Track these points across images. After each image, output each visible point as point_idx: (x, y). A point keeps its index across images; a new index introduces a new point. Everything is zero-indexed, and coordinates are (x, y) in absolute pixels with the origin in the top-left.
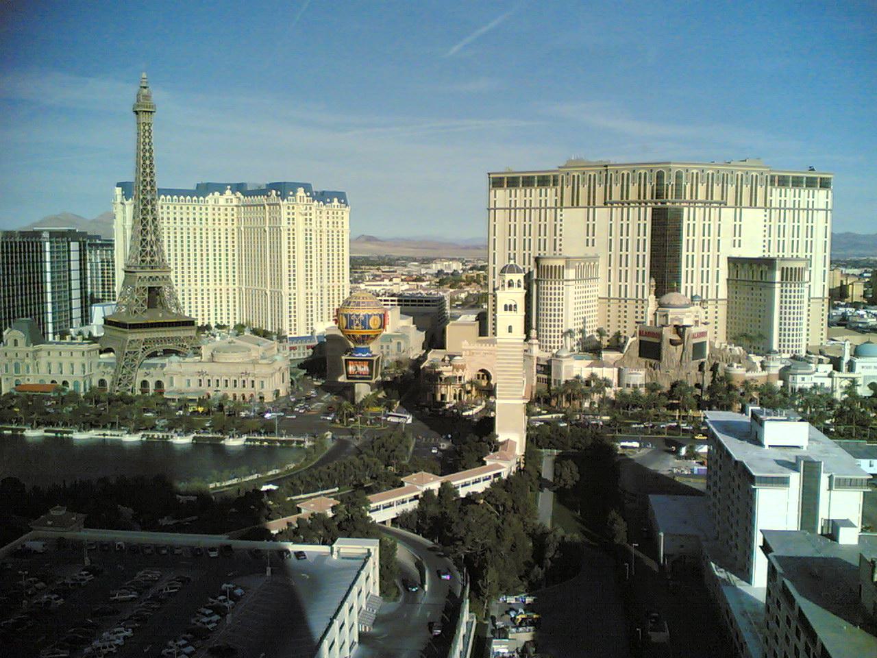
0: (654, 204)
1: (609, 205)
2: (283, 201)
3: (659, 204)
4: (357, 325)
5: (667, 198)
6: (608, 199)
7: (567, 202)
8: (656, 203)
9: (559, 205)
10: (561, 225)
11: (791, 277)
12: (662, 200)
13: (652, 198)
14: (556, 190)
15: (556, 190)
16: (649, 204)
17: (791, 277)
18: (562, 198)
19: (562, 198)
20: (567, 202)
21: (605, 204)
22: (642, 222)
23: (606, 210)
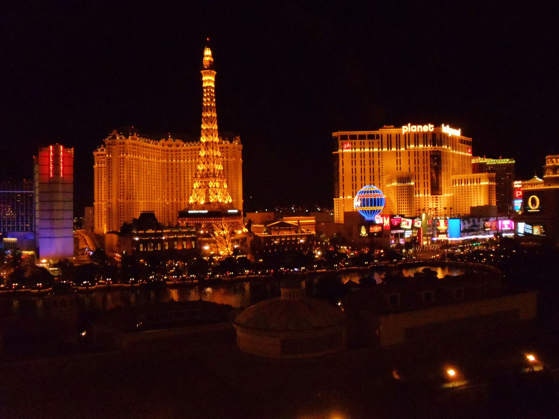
12: (435, 147)
14: (379, 142)
15: (379, 142)
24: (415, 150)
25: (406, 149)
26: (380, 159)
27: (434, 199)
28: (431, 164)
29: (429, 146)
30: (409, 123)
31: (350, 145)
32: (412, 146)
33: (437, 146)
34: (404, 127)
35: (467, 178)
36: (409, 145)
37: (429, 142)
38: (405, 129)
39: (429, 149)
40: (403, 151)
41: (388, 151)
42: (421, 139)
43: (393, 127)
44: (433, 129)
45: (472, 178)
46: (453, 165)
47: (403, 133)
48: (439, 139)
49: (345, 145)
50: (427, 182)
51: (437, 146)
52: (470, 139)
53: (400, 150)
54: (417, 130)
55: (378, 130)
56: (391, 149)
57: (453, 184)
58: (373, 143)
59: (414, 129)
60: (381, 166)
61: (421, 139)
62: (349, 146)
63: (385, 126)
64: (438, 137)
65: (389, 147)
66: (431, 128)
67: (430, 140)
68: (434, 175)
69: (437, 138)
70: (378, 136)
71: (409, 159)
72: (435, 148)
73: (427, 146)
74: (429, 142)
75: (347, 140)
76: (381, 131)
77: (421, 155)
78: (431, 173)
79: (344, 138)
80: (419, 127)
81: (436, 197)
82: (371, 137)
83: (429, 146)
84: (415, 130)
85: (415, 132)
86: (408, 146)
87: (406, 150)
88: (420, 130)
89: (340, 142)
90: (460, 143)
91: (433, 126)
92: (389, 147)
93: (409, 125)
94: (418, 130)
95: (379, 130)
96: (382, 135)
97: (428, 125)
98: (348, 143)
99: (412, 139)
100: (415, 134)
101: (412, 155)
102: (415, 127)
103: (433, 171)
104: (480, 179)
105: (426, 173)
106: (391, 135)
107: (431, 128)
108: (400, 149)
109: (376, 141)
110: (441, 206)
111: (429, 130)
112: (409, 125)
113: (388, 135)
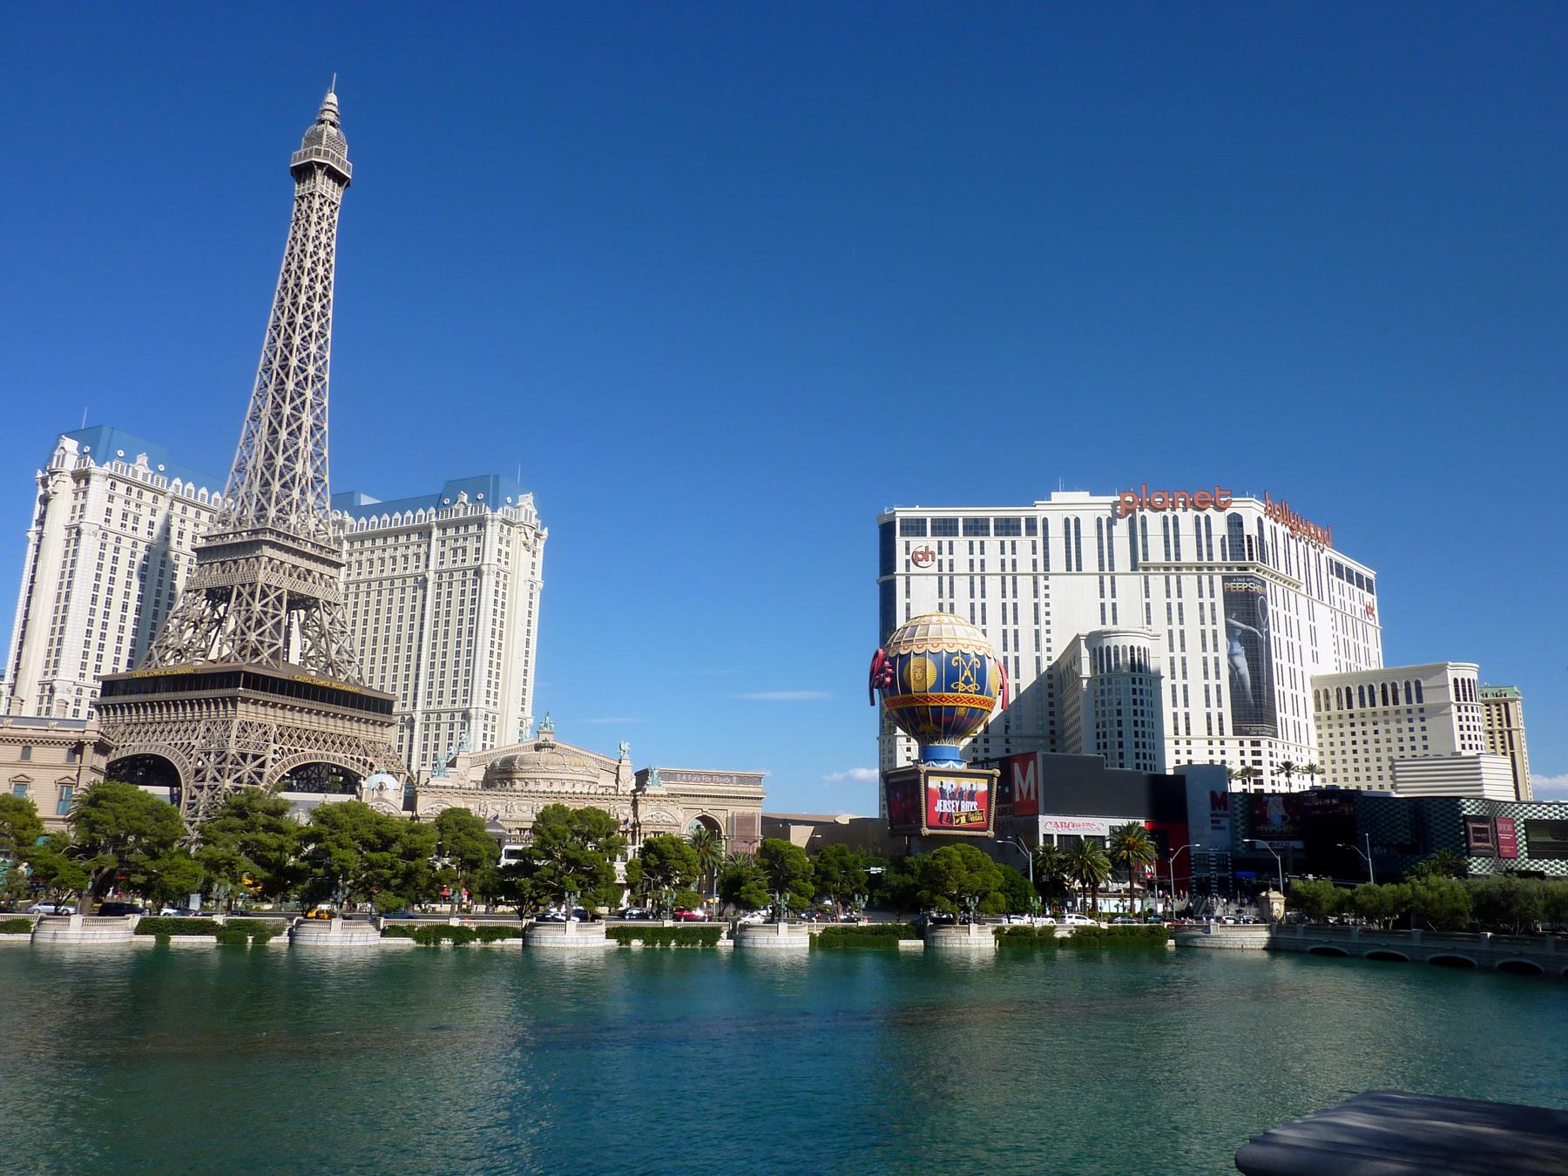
0: (1224, 571)
1: (1141, 571)
2: (495, 510)
3: (1235, 571)
4: (967, 681)
5: (1251, 559)
6: (1141, 559)
7: (1057, 563)
8: (1229, 568)
9: (1041, 568)
10: (1047, 605)
11: (1465, 695)
13: (1224, 558)
14: (1034, 543)
15: (1034, 543)
16: (1217, 571)
17: (1465, 695)
18: (1046, 556)
19: (1046, 556)
20: (1057, 563)
21: (1134, 566)
22: (1207, 600)
23: (1137, 580)
26: (1042, 601)
27: (1248, 748)
28: (1227, 624)
46: (1314, 641)
48: (1254, 532)
50: (1218, 687)
52: (1369, 573)
58: (1014, 548)
60: (1043, 627)
67: (1223, 540)
68: (1242, 662)
71: (1148, 605)
72: (1240, 569)
75: (924, 534)
78: (1231, 656)
81: (1254, 743)
82: (1007, 527)
90: (1332, 573)
96: (1045, 521)
103: (1239, 648)
106: (1077, 521)
109: (1024, 542)
110: (1274, 759)
113: (1067, 521)
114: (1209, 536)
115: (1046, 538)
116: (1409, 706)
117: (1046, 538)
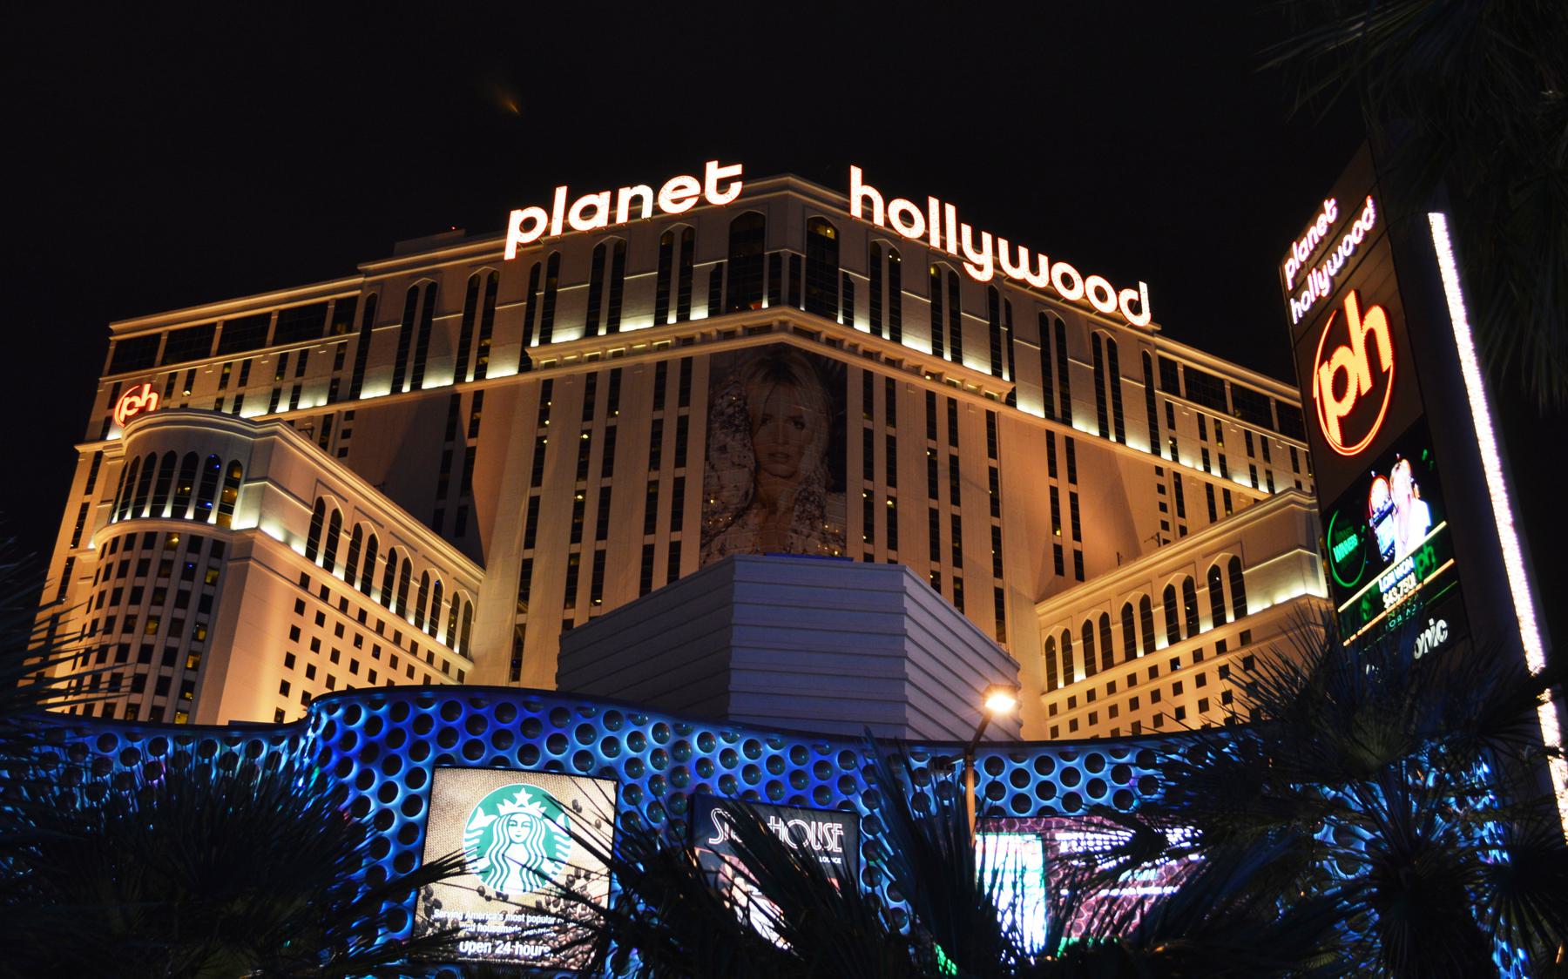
24: (594, 367)
25: (525, 365)
29: (699, 313)
30: (561, 185)
31: (154, 396)
32: (566, 335)
33: (765, 305)
34: (517, 217)
35: (1140, 594)
36: (545, 340)
37: (700, 287)
38: (528, 225)
39: (706, 339)
40: (508, 390)
41: (396, 398)
42: (641, 277)
43: (462, 232)
44: (736, 189)
45: (1176, 580)
47: (510, 254)
49: (127, 401)
51: (765, 305)
53: (480, 385)
54: (612, 218)
55: (355, 273)
56: (416, 386)
57: (1052, 686)
59: (589, 212)
61: (641, 277)
62: (148, 401)
63: (398, 245)
64: (789, 245)
65: (410, 365)
66: (723, 185)
67: (716, 273)
69: (766, 253)
70: (345, 308)
72: (751, 332)
73: (683, 316)
74: (700, 287)
76: (368, 274)
77: (638, 398)
79: (139, 355)
80: (625, 194)
83: (699, 313)
84: (600, 220)
85: (596, 233)
86: (535, 343)
87: (528, 377)
88: (634, 213)
89: (107, 382)
91: (737, 170)
92: (410, 365)
93: (561, 193)
94: (622, 217)
95: (358, 273)
97: (701, 179)
98: (147, 387)
99: (574, 289)
100: (602, 248)
101: (566, 407)
102: (602, 200)
104: (1235, 566)
105: (662, 539)
107: (723, 185)
108: (480, 374)
111: (702, 201)
112: (561, 193)
114: (687, 272)
115: (366, 336)
116: (1221, 634)
117: (366, 336)
